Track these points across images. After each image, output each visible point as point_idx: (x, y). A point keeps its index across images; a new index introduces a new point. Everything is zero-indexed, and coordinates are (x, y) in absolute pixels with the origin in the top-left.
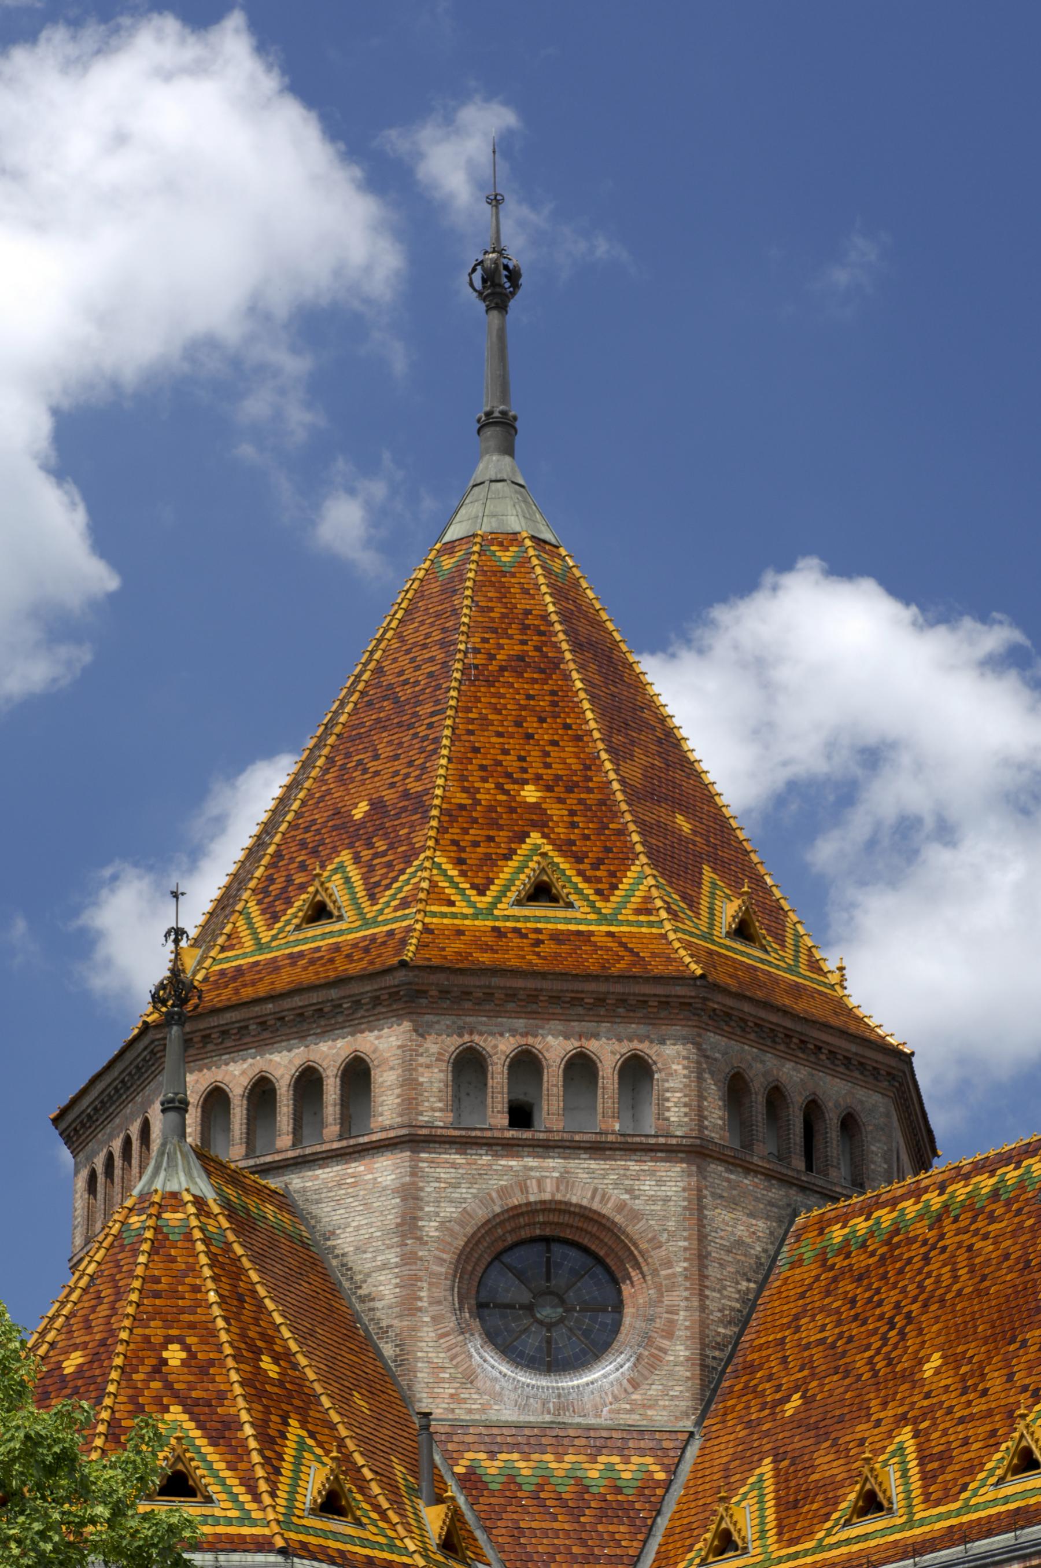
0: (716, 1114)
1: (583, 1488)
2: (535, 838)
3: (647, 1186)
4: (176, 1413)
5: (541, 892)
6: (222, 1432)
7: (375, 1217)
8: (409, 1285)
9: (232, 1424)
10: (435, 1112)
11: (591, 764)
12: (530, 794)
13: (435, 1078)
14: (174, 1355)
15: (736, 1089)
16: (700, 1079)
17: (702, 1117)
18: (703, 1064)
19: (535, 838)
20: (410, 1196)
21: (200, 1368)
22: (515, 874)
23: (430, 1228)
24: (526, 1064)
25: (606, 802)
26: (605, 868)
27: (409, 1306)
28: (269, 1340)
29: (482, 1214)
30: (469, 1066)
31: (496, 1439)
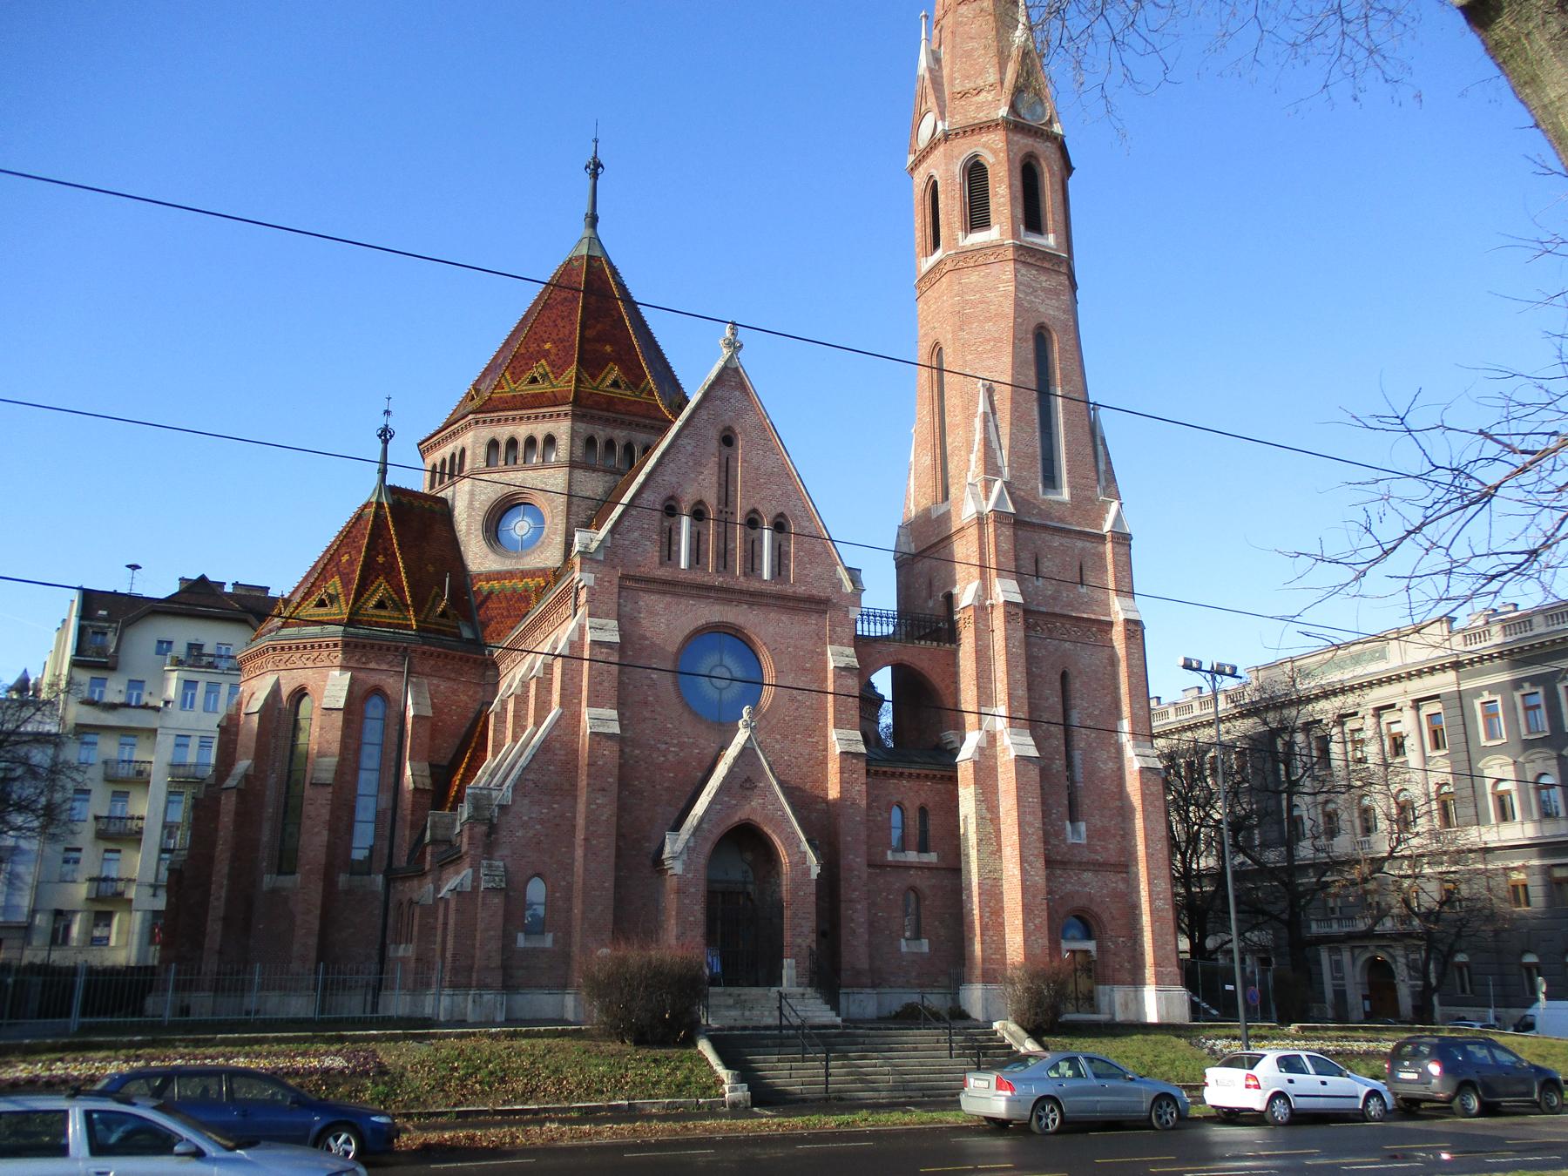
0: (579, 452)
1: (515, 590)
2: (543, 362)
3: (551, 481)
4: (337, 578)
5: (534, 380)
6: (346, 584)
7: (467, 502)
8: (468, 526)
9: (350, 581)
10: (482, 464)
11: (572, 333)
12: (548, 346)
13: (482, 451)
14: (345, 558)
15: (590, 442)
16: (572, 439)
17: (571, 453)
18: (574, 435)
19: (543, 362)
20: (472, 494)
21: (351, 562)
22: (528, 376)
23: (477, 504)
24: (512, 443)
25: (573, 346)
26: (558, 369)
27: (468, 533)
28: (386, 549)
29: (494, 497)
30: (493, 445)
31: (489, 577)
